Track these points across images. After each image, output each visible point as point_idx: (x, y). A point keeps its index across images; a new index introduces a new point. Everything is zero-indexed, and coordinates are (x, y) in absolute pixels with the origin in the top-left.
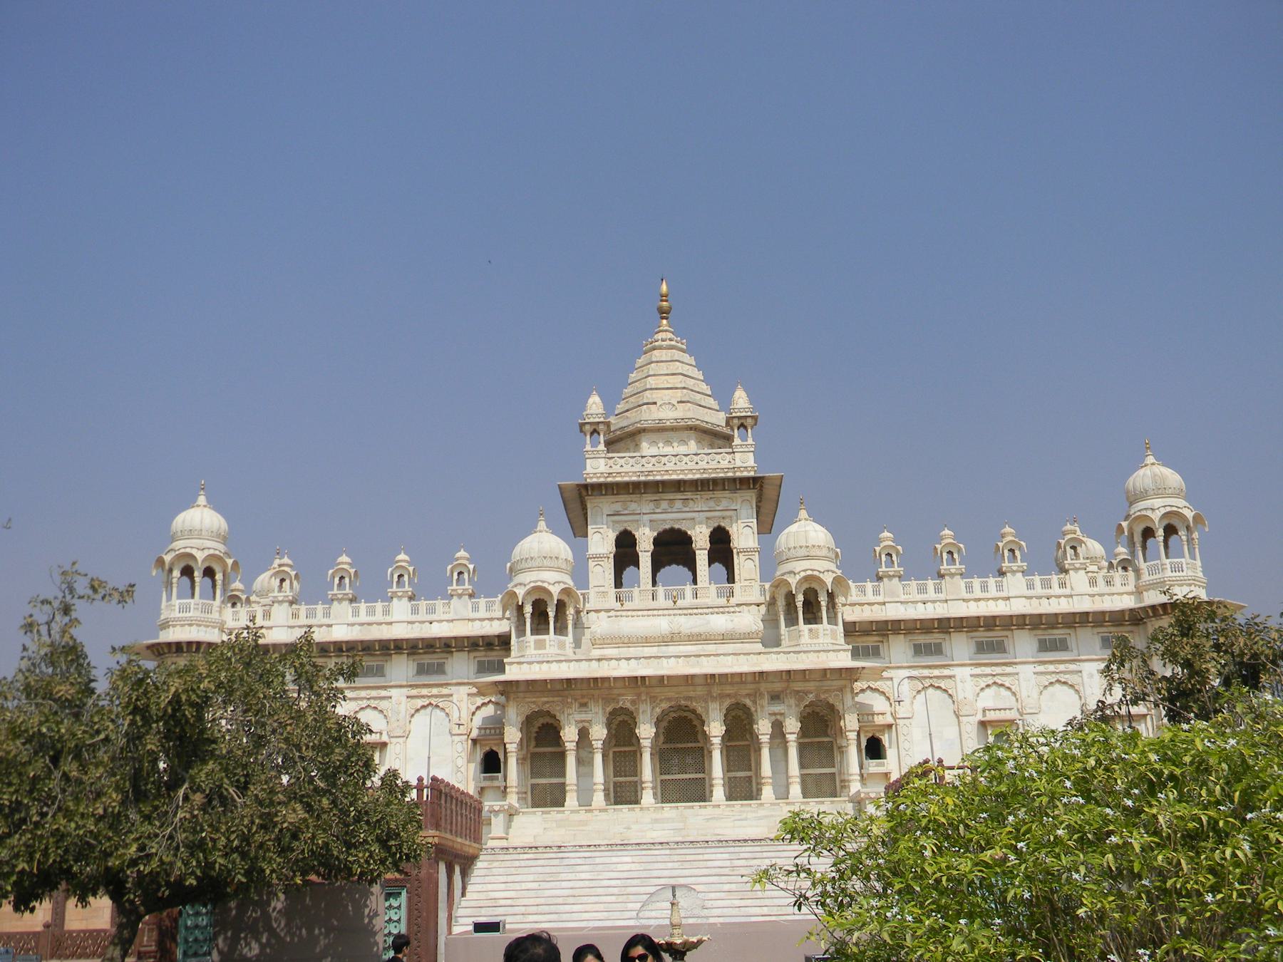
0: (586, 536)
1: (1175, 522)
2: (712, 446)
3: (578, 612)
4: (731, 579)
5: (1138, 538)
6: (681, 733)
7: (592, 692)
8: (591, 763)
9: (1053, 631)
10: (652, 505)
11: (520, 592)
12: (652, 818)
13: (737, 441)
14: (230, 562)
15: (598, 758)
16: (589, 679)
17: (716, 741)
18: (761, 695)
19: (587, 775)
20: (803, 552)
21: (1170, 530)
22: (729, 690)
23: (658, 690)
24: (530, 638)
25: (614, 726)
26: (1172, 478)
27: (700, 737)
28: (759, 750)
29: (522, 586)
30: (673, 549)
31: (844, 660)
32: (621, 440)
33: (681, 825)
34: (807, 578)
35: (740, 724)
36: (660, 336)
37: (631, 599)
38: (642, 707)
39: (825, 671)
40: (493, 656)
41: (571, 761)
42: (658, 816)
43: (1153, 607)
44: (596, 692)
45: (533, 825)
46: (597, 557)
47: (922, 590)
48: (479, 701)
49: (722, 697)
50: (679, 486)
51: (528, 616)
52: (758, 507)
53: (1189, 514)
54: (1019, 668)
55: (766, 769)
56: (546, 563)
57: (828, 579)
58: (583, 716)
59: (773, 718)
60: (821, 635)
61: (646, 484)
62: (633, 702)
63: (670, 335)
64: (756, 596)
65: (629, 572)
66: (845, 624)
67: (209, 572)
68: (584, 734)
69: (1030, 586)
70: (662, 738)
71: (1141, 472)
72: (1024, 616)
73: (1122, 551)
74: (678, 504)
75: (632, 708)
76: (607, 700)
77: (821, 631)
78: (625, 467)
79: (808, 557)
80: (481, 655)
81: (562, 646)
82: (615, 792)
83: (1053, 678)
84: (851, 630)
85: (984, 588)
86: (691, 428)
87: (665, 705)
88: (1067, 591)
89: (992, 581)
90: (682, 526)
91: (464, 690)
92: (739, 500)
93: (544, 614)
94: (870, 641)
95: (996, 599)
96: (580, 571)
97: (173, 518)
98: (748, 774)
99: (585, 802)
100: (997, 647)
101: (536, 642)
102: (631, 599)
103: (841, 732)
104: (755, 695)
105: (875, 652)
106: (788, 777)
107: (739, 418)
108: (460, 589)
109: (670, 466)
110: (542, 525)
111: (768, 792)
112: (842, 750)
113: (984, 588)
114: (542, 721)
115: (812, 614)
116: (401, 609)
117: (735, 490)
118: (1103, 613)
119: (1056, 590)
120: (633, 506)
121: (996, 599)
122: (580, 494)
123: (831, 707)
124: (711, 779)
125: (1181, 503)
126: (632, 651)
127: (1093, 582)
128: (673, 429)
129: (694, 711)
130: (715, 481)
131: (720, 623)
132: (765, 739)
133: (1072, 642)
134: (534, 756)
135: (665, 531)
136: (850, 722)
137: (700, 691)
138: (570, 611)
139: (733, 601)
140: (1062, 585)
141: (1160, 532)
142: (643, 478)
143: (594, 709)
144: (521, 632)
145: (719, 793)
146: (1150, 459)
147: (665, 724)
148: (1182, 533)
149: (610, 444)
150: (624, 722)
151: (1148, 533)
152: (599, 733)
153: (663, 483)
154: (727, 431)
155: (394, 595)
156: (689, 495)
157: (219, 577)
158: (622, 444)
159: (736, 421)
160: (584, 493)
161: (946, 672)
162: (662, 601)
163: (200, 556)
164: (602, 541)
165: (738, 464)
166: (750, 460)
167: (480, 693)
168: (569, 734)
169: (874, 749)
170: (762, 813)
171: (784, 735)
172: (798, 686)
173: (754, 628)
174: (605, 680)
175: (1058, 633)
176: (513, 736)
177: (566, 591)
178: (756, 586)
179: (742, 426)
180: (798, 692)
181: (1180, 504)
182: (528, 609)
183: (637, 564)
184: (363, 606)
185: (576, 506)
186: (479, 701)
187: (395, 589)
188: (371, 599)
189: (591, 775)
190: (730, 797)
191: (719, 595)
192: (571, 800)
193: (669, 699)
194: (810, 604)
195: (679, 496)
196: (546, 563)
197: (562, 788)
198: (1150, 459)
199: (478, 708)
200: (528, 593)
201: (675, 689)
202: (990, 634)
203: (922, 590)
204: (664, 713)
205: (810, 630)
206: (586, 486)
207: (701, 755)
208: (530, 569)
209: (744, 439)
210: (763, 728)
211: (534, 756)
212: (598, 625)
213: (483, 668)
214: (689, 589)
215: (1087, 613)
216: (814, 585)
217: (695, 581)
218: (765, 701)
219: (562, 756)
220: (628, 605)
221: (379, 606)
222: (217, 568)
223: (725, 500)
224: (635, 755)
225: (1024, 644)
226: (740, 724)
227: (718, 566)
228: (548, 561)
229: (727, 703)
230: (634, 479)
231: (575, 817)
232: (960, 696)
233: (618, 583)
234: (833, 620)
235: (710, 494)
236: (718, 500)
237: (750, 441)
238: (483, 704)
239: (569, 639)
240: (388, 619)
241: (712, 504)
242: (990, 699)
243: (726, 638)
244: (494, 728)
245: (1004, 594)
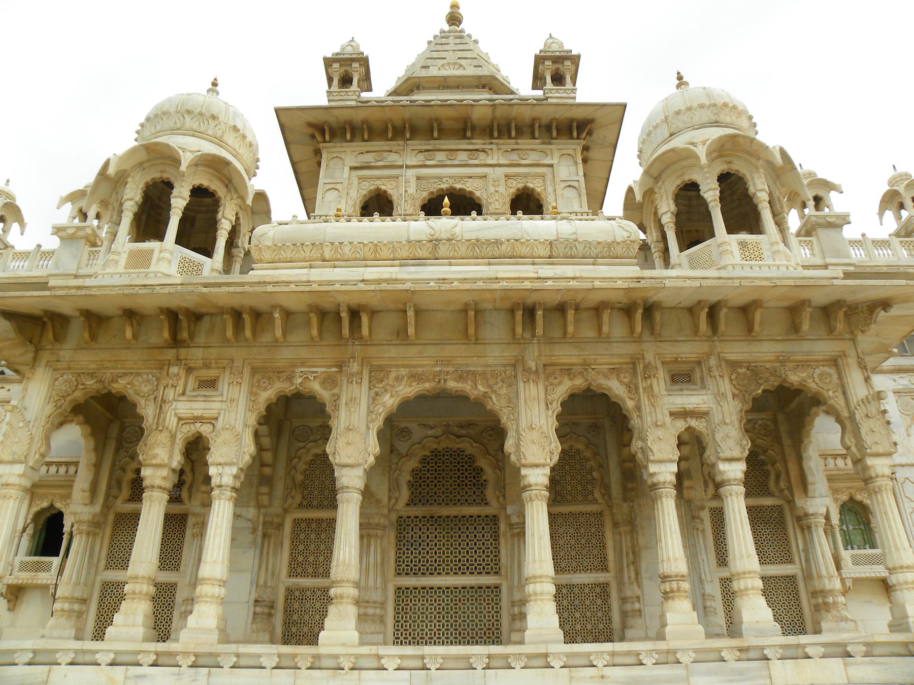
6: (448, 475)
7: (231, 352)
10: (421, 157)
17: (537, 477)
18: (648, 372)
20: (706, 116)
23: (393, 352)
25: (301, 466)
27: (490, 493)
44: (238, 354)
49: (550, 371)
56: (189, 122)
58: (198, 408)
59: (681, 425)
60: (766, 254)
62: (329, 381)
70: (405, 494)
75: (324, 394)
77: (765, 246)
82: (288, 611)
87: (408, 390)
92: (556, 155)
98: (601, 577)
99: (162, 626)
101: (132, 254)
111: (681, 615)
120: (393, 158)
124: (523, 582)
137: (496, 354)
143: (234, 392)
145: (543, 618)
147: (413, 463)
156: (478, 143)
159: (548, 63)
160: (319, 138)
172: (737, 351)
180: (734, 365)
195: (464, 144)
196: (189, 122)
201: (431, 351)
205: (743, 245)
207: (488, 536)
216: (739, 166)
218: (660, 383)
223: (532, 152)
229: (563, 389)
235: (510, 144)
241: (514, 157)
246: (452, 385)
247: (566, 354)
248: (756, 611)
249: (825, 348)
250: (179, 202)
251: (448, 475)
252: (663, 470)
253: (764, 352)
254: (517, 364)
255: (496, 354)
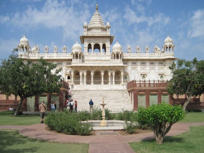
0: (84, 43)
1: (171, 46)
2: (103, 31)
3: (83, 56)
4: (105, 51)
5: (165, 48)
6: (97, 74)
8: (84, 78)
9: (152, 62)
11: (74, 52)
12: (93, 87)
13: (107, 30)
14: (29, 46)
15: (85, 78)
16: (84, 66)
17: (103, 76)
19: (83, 80)
20: (116, 48)
21: (170, 47)
22: (105, 68)
24: (75, 60)
26: (171, 39)
28: (109, 77)
29: (74, 51)
30: (97, 46)
31: (122, 64)
32: (89, 29)
33: (97, 88)
34: (117, 52)
35: (106, 73)
36: (96, 13)
37: (90, 54)
38: (92, 70)
39: (119, 66)
40: (70, 62)
41: (81, 78)
42: (94, 86)
43: (167, 59)
45: (76, 87)
46: (85, 47)
47: (134, 54)
48: (67, 69)
49: (103, 69)
50: (98, 37)
51: (75, 56)
52: (110, 41)
53: (173, 45)
54: (147, 67)
55: (110, 80)
57: (120, 53)
61: (93, 36)
63: (97, 13)
64: (109, 55)
65: (90, 49)
66: (122, 59)
67: (26, 48)
68: (83, 74)
69: (150, 55)
71: (167, 38)
72: (148, 59)
73: (163, 50)
74: (98, 40)
76: (87, 69)
78: (90, 34)
79: (118, 49)
80: (68, 62)
81: (80, 61)
83: (151, 68)
84: (123, 60)
85: (143, 55)
86: (100, 28)
88: (155, 56)
89: (144, 54)
90: (99, 43)
91: (65, 67)
93: (76, 56)
94: (126, 62)
95: (144, 56)
96: (82, 49)
97: (20, 39)
100: (144, 63)
102: (90, 54)
103: (121, 75)
104: (108, 69)
105: (126, 63)
106: (113, 81)
107: (108, 27)
108: (64, 52)
109: (97, 34)
110: (77, 42)
111: (110, 83)
112: (121, 78)
113: (143, 55)
114: (76, 72)
115: (118, 57)
116: (55, 54)
117: (107, 38)
118: (159, 59)
119: (153, 55)
120: (91, 40)
121: (144, 56)
122: (83, 38)
123: (120, 71)
125: (171, 44)
126: (91, 62)
127: (158, 54)
128: (98, 28)
129: (99, 71)
130: (104, 36)
131: (104, 58)
132: (110, 76)
133: (155, 63)
134: (75, 77)
135: (96, 44)
136: (122, 74)
137: (101, 68)
138: (81, 56)
139: (106, 55)
140: (154, 55)
141: (168, 48)
142: (93, 36)
144: (74, 59)
145: (103, 83)
146: (168, 37)
148: (172, 48)
149: (88, 30)
150: (89, 73)
151: (167, 48)
152: (85, 74)
153: (96, 36)
154: (106, 29)
155: (54, 52)
157: (27, 49)
158: (89, 30)
161: (137, 67)
162: (95, 55)
163: (25, 45)
164: (86, 45)
165: (107, 34)
166: (109, 34)
167: (68, 67)
168: (81, 74)
169: (126, 77)
170: (109, 86)
171: (112, 75)
172: (115, 68)
173: (109, 59)
174: (86, 66)
175: (153, 62)
176: (72, 74)
177: (81, 53)
178: (109, 53)
179: (108, 28)
181: (171, 44)
182: (75, 56)
183: (91, 49)
184: (49, 54)
185: (82, 39)
186: (67, 69)
187: (54, 51)
188: (51, 53)
189: (84, 80)
190: (104, 84)
191: (104, 54)
192: (81, 83)
193: (96, 69)
194: (117, 56)
197: (80, 82)
198: (168, 37)
199: (67, 70)
200: (75, 53)
202: (143, 62)
203: (134, 54)
204: (95, 71)
206: (84, 36)
207: (100, 77)
208: (75, 49)
209: (108, 30)
210: (109, 74)
211: (75, 77)
212: (86, 58)
213: (68, 64)
214: (99, 53)
215: (157, 59)
216: (118, 53)
217: (100, 52)
218: (110, 70)
219: (80, 77)
220: (90, 55)
221: (52, 54)
222: (27, 47)
223: (105, 39)
224: (90, 78)
225: (148, 63)
226: (106, 73)
227: (104, 50)
228: (78, 48)
230: (92, 36)
231: (82, 86)
232: (138, 70)
233: (88, 52)
234: (121, 59)
235: (102, 38)
236: (104, 39)
237: (109, 30)
238: (68, 69)
239: (81, 60)
240: (53, 56)
242: (142, 71)
243: (105, 60)
244: (70, 73)
245: (146, 56)
246: (98, 70)
247: (105, 68)
248: (114, 83)
249: (121, 68)
250: (78, 55)
251: (97, 74)
252: (110, 76)
253: (117, 68)
254: (102, 69)
255: (101, 68)
